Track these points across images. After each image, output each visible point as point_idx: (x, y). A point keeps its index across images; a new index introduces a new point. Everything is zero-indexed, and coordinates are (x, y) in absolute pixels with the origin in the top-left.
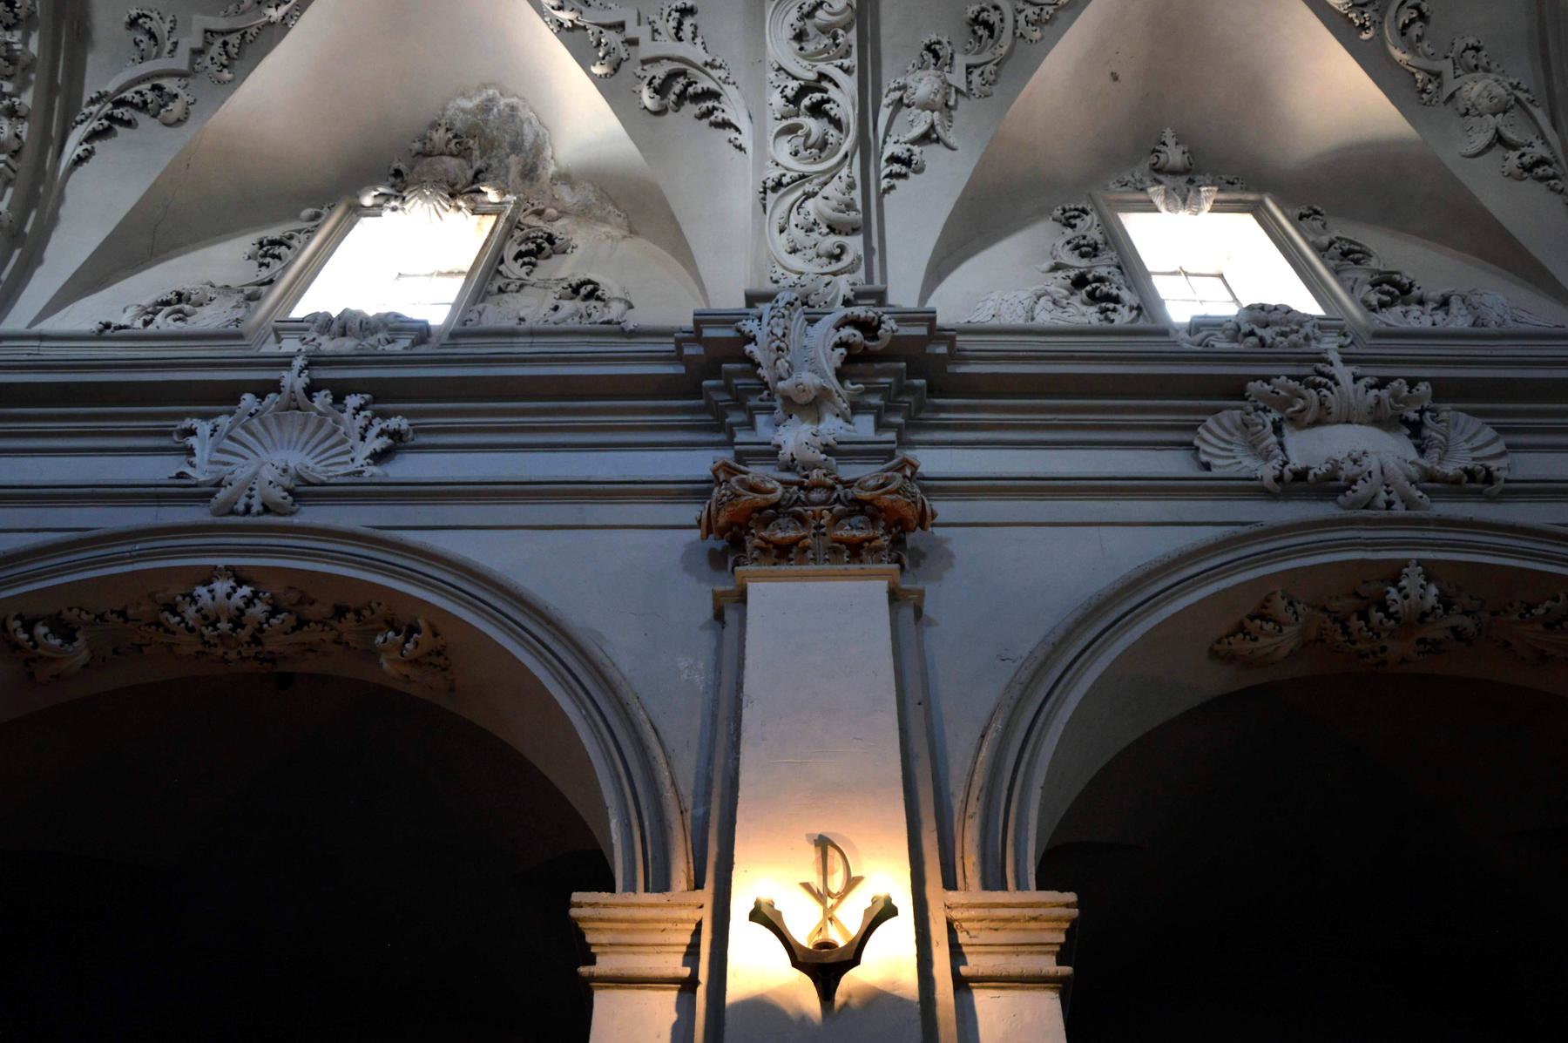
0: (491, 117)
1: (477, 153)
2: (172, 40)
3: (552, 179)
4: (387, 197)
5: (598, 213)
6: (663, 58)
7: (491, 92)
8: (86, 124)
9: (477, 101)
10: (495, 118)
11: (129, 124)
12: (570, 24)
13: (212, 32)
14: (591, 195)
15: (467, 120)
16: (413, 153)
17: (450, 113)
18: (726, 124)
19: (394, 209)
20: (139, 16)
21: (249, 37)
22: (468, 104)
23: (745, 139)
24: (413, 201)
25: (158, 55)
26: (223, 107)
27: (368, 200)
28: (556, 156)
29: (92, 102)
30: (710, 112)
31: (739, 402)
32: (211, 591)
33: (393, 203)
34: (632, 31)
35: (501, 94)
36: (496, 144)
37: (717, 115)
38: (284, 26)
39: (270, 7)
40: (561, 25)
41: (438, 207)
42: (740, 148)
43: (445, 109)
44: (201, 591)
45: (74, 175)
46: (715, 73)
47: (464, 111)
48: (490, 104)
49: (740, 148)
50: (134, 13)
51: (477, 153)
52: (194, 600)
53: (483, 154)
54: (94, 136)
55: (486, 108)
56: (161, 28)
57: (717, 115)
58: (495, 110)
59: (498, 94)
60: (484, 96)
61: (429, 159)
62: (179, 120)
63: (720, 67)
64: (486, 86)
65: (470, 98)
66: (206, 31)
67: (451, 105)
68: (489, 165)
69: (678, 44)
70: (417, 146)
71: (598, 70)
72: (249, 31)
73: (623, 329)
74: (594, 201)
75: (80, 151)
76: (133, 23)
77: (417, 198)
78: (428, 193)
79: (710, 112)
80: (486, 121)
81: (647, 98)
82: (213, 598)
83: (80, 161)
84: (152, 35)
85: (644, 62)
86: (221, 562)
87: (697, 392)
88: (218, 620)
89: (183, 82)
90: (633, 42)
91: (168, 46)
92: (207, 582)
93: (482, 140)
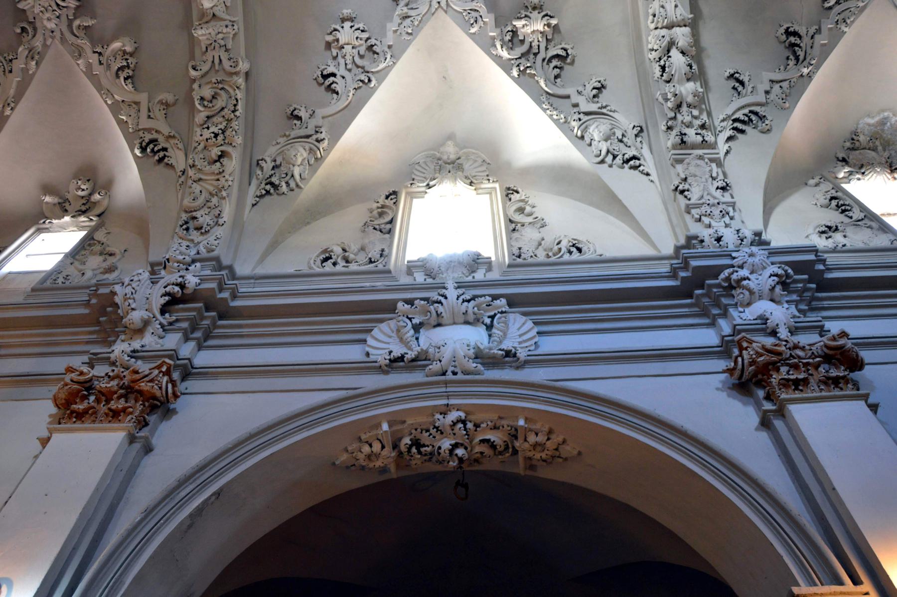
0: (886, 128)
1: (880, 148)
2: (751, 86)
4: (851, 173)
7: (886, 114)
8: (723, 132)
9: (877, 119)
10: (889, 128)
11: (742, 132)
13: (772, 81)
15: (871, 130)
16: (846, 148)
17: (861, 126)
19: (859, 179)
20: (735, 73)
21: (792, 84)
22: (871, 121)
24: (871, 175)
25: (746, 95)
26: (789, 122)
27: (841, 175)
29: (723, 121)
33: (858, 176)
35: (894, 115)
36: (891, 143)
38: (810, 76)
39: (805, 67)
41: (885, 177)
43: (858, 124)
45: (726, 160)
47: (869, 125)
48: (885, 121)
50: (732, 72)
51: (880, 148)
53: (884, 150)
54: (730, 139)
55: (883, 123)
56: (746, 79)
58: (889, 124)
59: (891, 115)
60: (882, 116)
61: (858, 152)
62: (768, 130)
64: (883, 111)
65: (873, 117)
66: (770, 81)
67: (861, 122)
68: (891, 154)
70: (848, 144)
72: (792, 81)
75: (726, 147)
76: (731, 76)
77: (872, 173)
78: (879, 170)
80: (883, 130)
83: (727, 152)
84: (742, 83)
89: (763, 109)
91: (750, 89)
93: (882, 141)
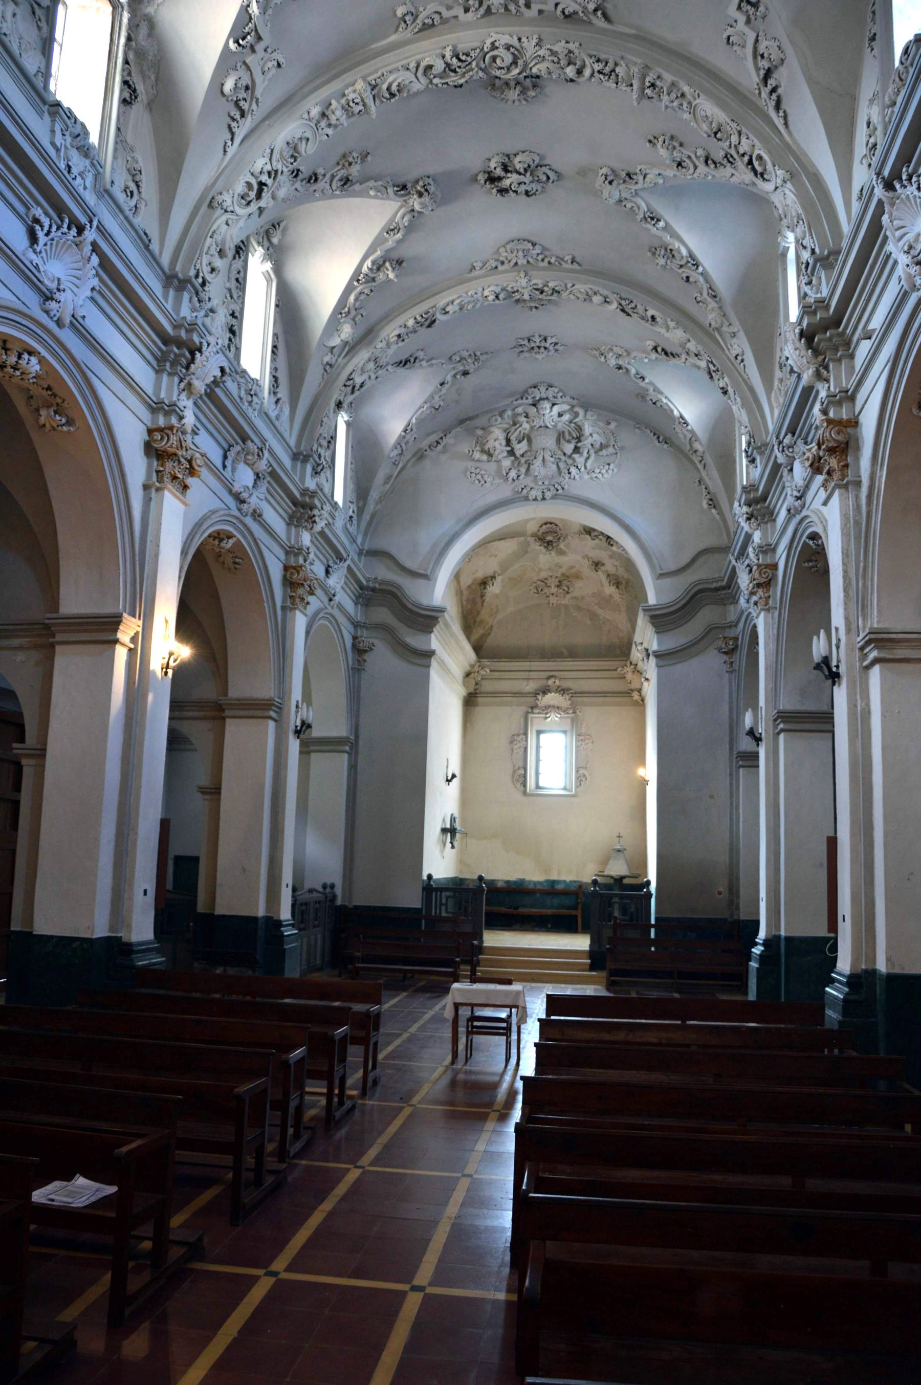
3: (145, 15)
5: (145, 68)
6: (250, 71)
12: (251, 12)
14: (151, 53)
18: (233, 134)
23: (231, 150)
28: (161, 7)
30: (233, 119)
31: (174, 364)
32: (29, 360)
34: (259, 47)
37: (234, 124)
40: (248, 6)
42: (225, 151)
44: (26, 356)
46: (254, 106)
49: (225, 151)
52: (19, 357)
57: (234, 124)
63: (258, 105)
69: (261, 74)
71: (232, 46)
73: (148, 246)
74: (150, 58)
79: (233, 119)
81: (229, 86)
82: (28, 363)
85: (245, 63)
86: (44, 353)
87: (165, 343)
88: (18, 369)
90: (253, 50)
92: (30, 354)
